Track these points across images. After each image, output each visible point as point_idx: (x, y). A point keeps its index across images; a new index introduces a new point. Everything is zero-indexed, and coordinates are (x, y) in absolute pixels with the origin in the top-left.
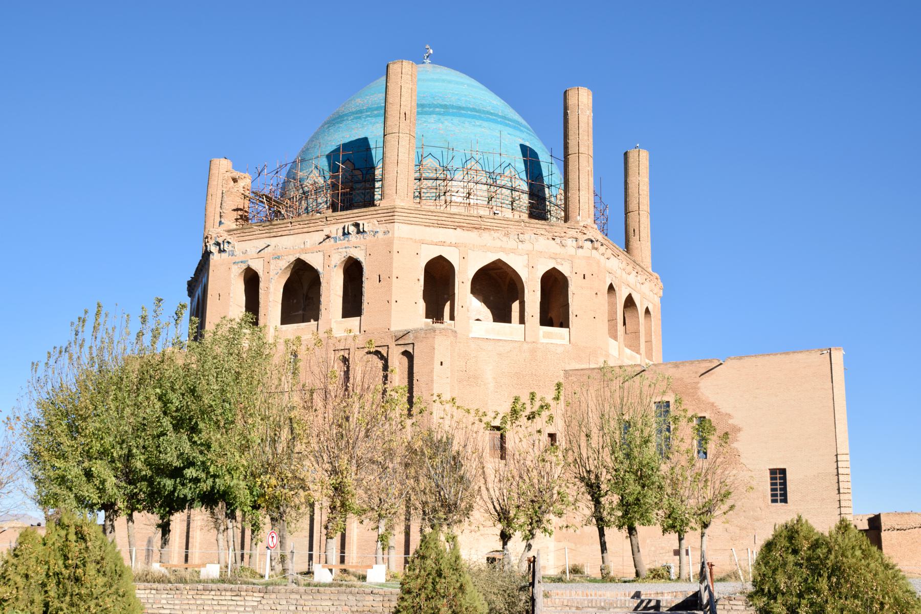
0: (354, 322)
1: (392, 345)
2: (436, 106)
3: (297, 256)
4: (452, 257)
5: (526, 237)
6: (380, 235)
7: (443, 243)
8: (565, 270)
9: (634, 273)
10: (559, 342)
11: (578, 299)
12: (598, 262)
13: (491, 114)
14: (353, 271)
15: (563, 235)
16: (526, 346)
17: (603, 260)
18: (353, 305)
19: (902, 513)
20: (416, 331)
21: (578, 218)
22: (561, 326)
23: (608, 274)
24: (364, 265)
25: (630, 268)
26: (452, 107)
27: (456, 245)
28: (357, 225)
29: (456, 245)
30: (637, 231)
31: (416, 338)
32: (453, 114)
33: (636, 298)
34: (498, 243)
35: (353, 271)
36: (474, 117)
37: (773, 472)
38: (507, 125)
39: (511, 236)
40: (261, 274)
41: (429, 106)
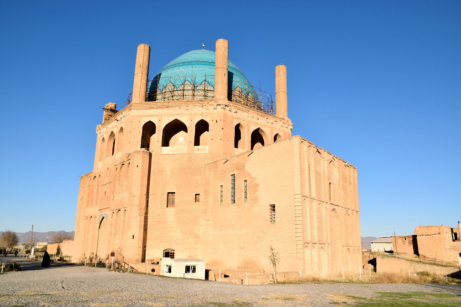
1: (126, 160)
2: (181, 63)
5: (190, 107)
7: (151, 116)
10: (203, 152)
12: (225, 115)
13: (205, 62)
15: (207, 104)
16: (186, 156)
19: (428, 226)
21: (217, 96)
23: (235, 120)
26: (187, 62)
27: (157, 116)
29: (157, 116)
32: (186, 65)
34: (177, 112)
37: (271, 206)
38: (210, 65)
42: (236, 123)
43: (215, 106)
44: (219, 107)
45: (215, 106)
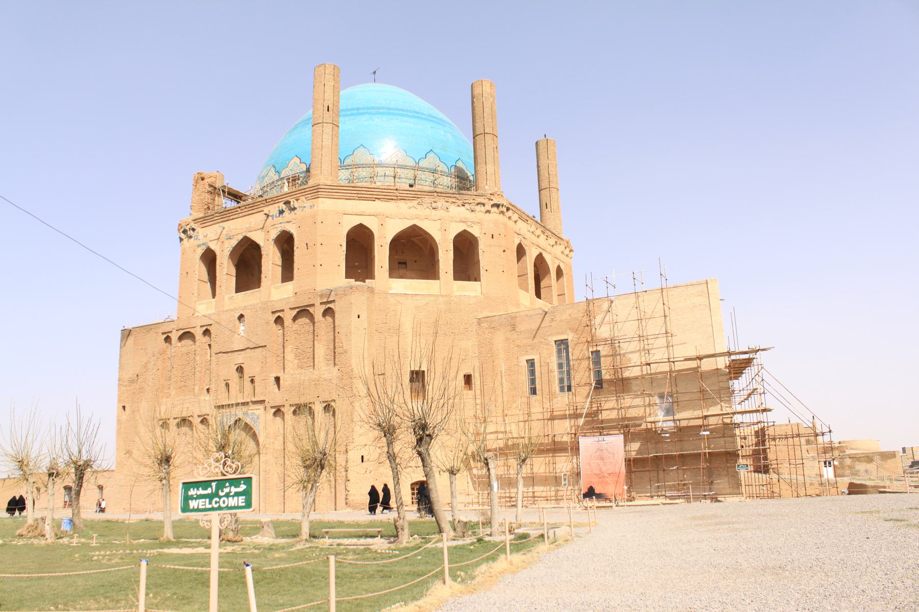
0: (289, 285)
1: (317, 302)
3: (244, 234)
4: (371, 223)
5: (439, 204)
6: (308, 211)
8: (475, 231)
9: (543, 237)
10: (473, 294)
11: (486, 255)
12: (505, 225)
13: (417, 113)
14: (286, 242)
16: (441, 299)
17: (511, 224)
18: (288, 273)
20: (336, 289)
22: (476, 280)
24: (295, 236)
25: (538, 232)
28: (287, 203)
30: (549, 205)
31: (336, 295)
32: (383, 114)
33: (547, 257)
35: (286, 242)
36: (401, 115)
39: (425, 205)
40: (218, 253)
41: (364, 109)
42: (517, 242)
43: (488, 207)
44: (495, 209)
45: (488, 207)
